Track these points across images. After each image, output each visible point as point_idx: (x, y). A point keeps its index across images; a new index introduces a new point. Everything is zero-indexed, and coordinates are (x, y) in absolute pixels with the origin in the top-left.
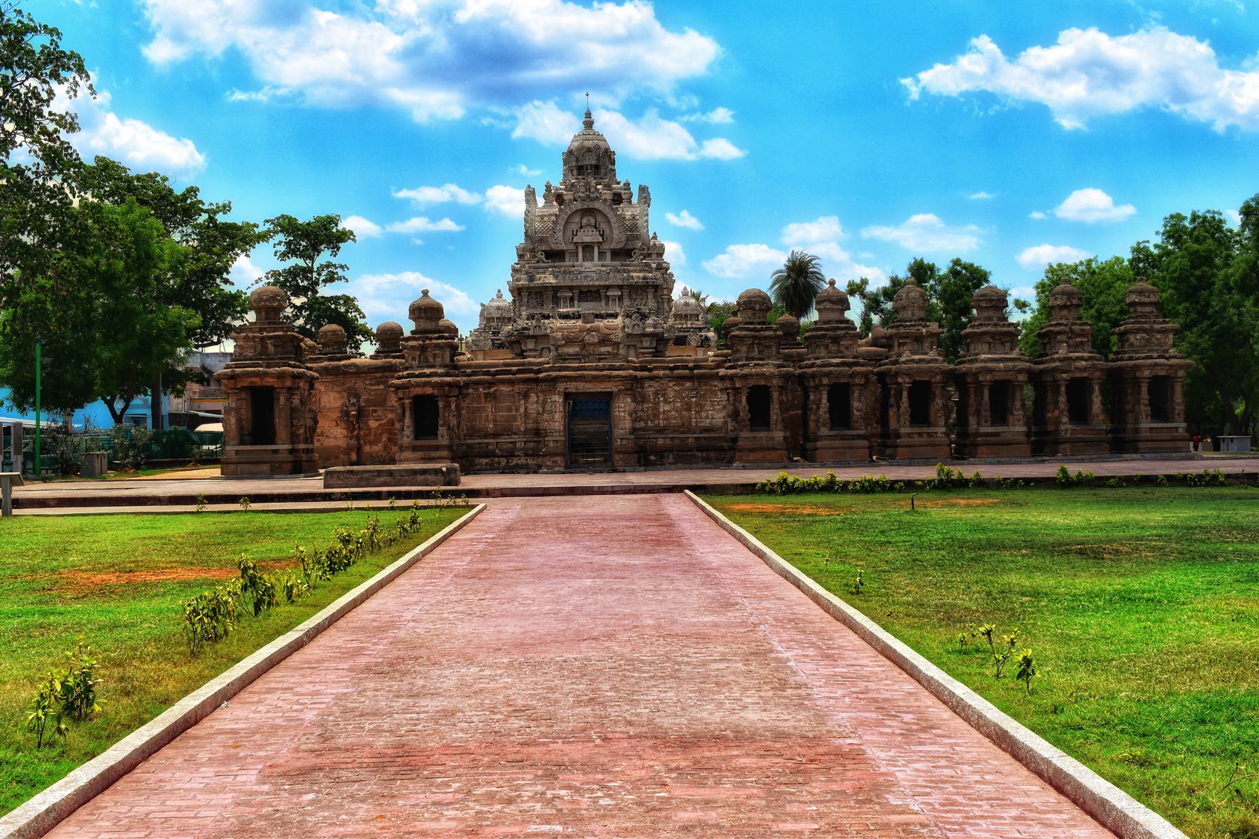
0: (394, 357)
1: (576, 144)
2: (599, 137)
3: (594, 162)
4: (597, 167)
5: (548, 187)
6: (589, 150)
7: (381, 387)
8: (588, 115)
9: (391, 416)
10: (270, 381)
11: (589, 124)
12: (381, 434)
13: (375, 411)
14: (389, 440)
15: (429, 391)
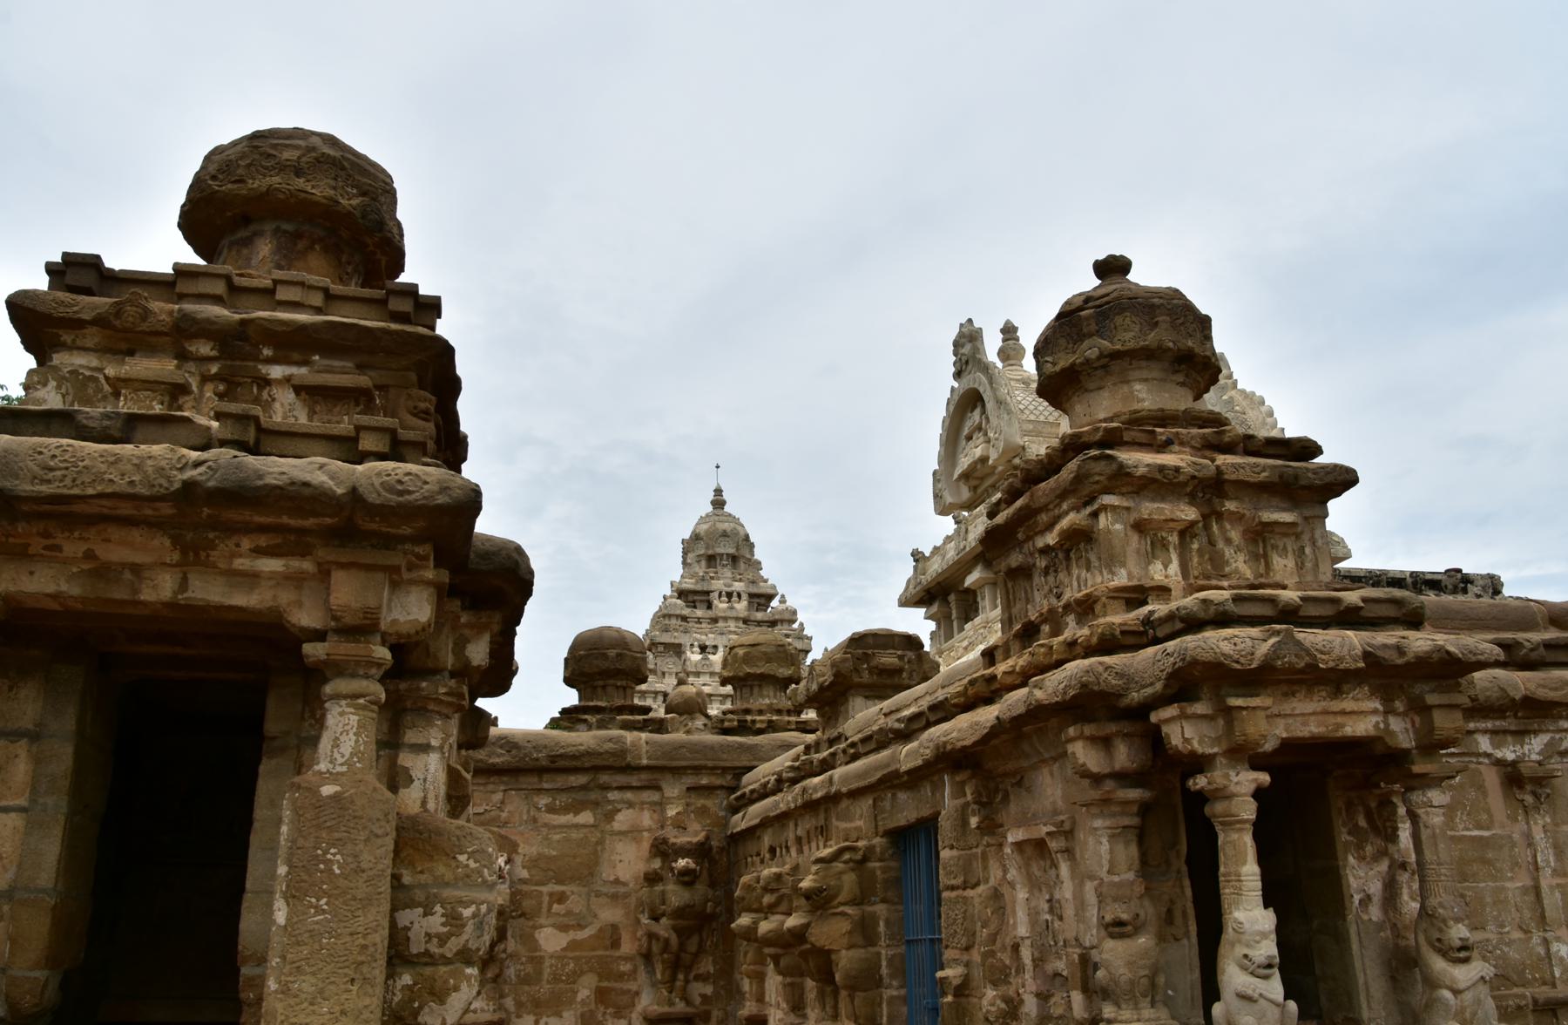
0: (627, 726)
1: (705, 527)
2: (736, 520)
3: (732, 551)
4: (734, 559)
5: (1009, 331)
6: (725, 534)
7: (586, 817)
8: (718, 492)
9: (610, 914)
10: (255, 582)
11: (719, 503)
12: (575, 976)
13: (561, 898)
14: (601, 995)
15: (1361, 717)
